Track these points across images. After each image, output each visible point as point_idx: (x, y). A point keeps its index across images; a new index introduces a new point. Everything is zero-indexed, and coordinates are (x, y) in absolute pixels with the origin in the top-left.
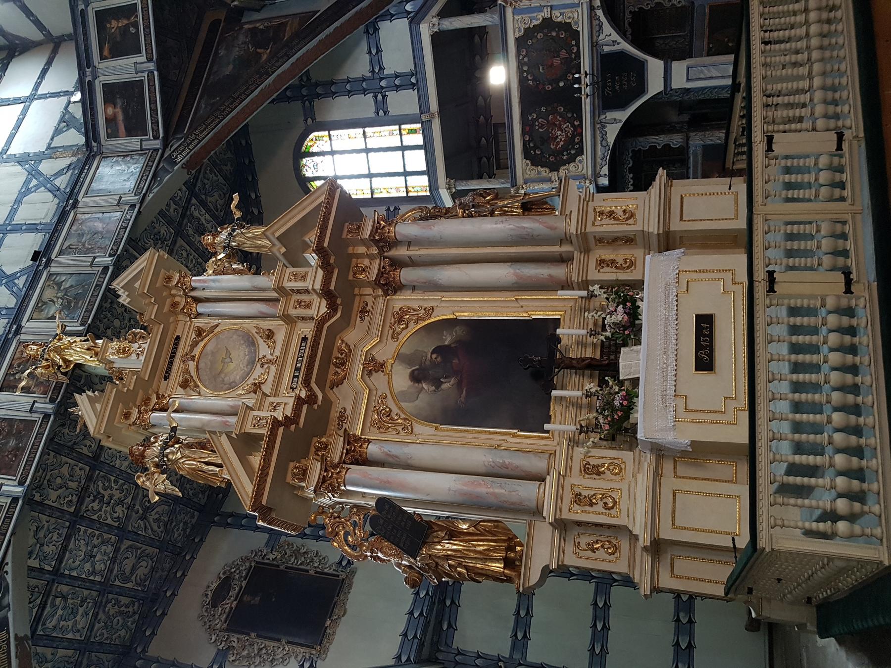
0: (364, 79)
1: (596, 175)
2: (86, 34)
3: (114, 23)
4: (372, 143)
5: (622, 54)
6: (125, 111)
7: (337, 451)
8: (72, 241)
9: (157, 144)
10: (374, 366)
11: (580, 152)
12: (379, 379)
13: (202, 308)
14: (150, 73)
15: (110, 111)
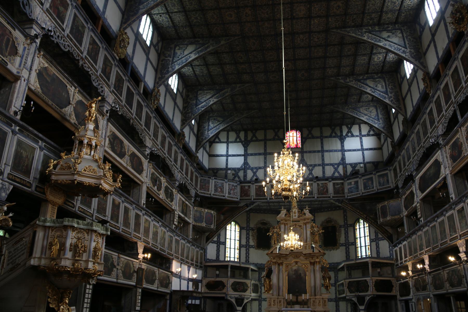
0: (378, 236)
1: (348, 296)
2: (368, 175)
3: (370, 182)
4: (366, 237)
5: (365, 301)
6: (353, 187)
7: (279, 262)
8: (321, 185)
9: (346, 197)
10: (296, 263)
11: (350, 293)
12: (294, 264)
13: (304, 226)
14: (360, 194)
15: (353, 183)
